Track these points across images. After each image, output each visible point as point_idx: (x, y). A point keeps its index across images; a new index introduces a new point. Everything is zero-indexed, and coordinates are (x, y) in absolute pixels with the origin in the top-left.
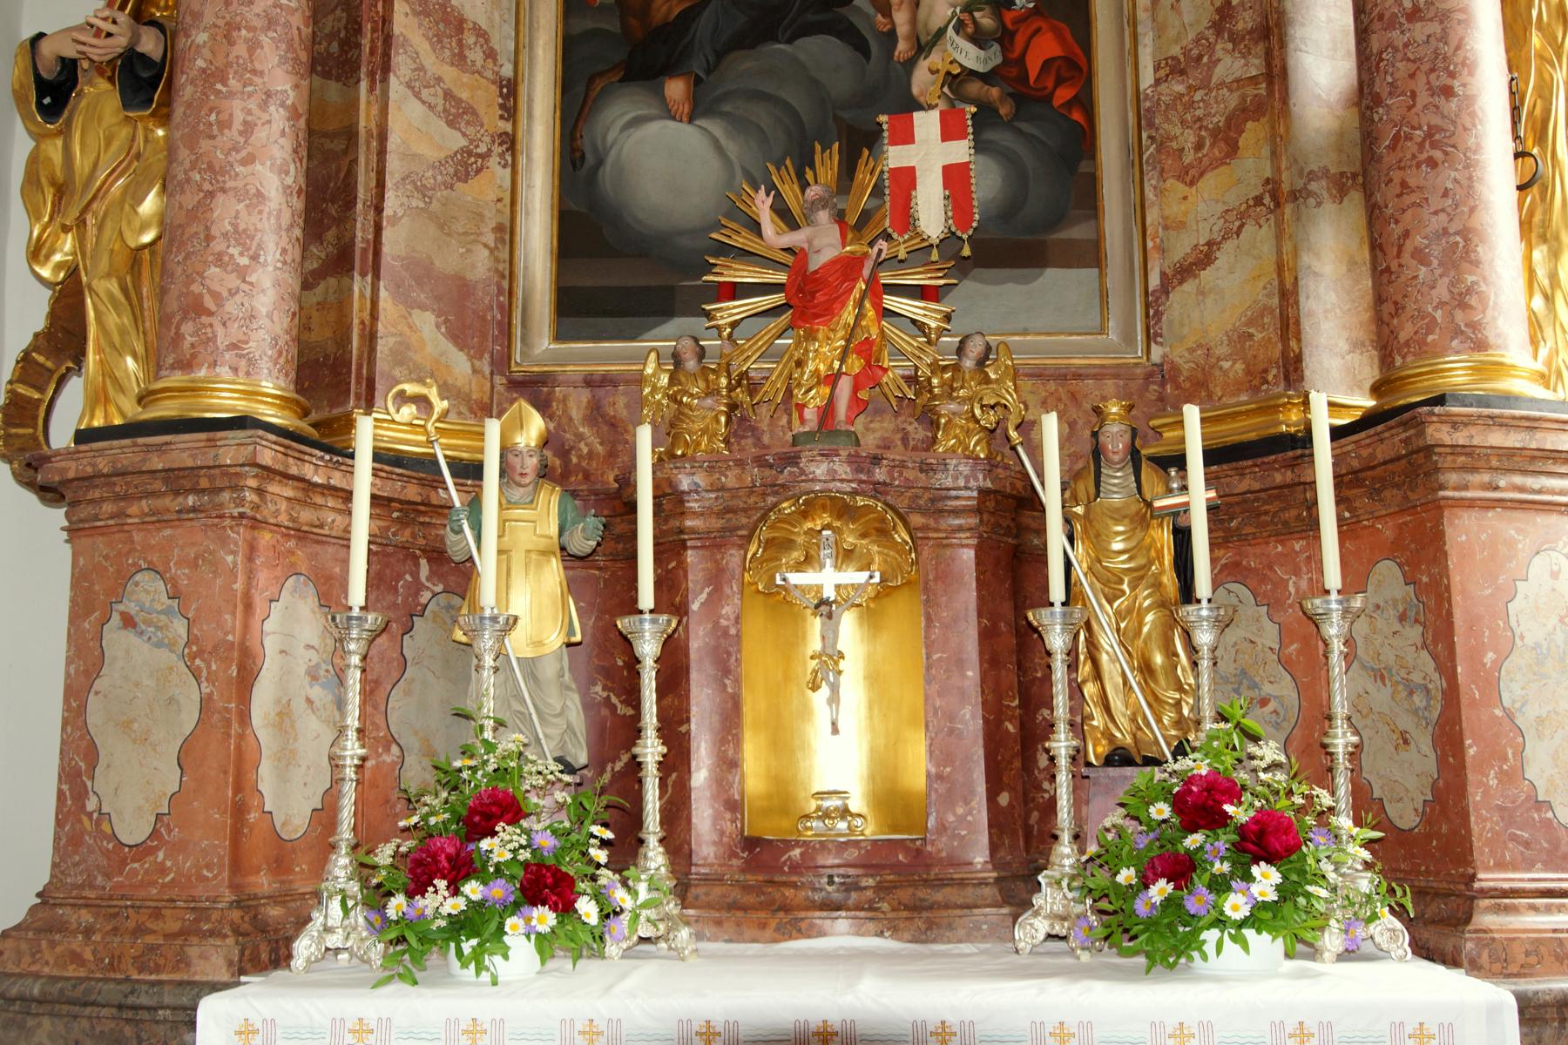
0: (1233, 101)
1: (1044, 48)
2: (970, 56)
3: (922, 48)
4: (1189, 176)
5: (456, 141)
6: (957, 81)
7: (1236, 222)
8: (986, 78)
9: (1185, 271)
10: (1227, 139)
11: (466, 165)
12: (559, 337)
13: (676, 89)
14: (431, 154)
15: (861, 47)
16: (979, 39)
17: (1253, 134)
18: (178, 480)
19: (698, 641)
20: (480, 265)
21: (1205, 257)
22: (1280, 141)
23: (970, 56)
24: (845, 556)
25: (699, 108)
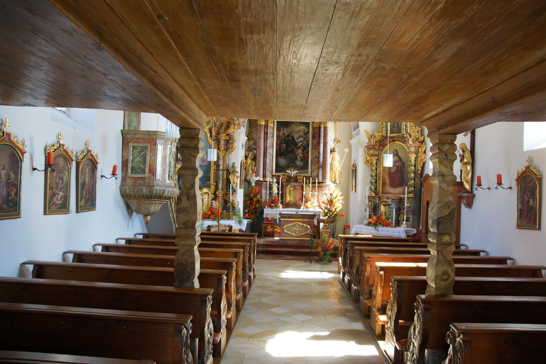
0: (316, 162)
1: (306, 155)
2: (301, 155)
3: (298, 155)
4: (314, 165)
5: (270, 161)
6: (300, 157)
7: (316, 169)
8: (302, 157)
9: (313, 171)
10: (316, 163)
11: (270, 163)
12: (275, 173)
13: (283, 157)
14: (269, 162)
15: (294, 154)
16: (302, 154)
17: (317, 164)
18: (259, 184)
19: (284, 192)
20: (271, 169)
21: (314, 171)
22: (319, 165)
23: (301, 155)
24: (292, 188)
25: (284, 158)
